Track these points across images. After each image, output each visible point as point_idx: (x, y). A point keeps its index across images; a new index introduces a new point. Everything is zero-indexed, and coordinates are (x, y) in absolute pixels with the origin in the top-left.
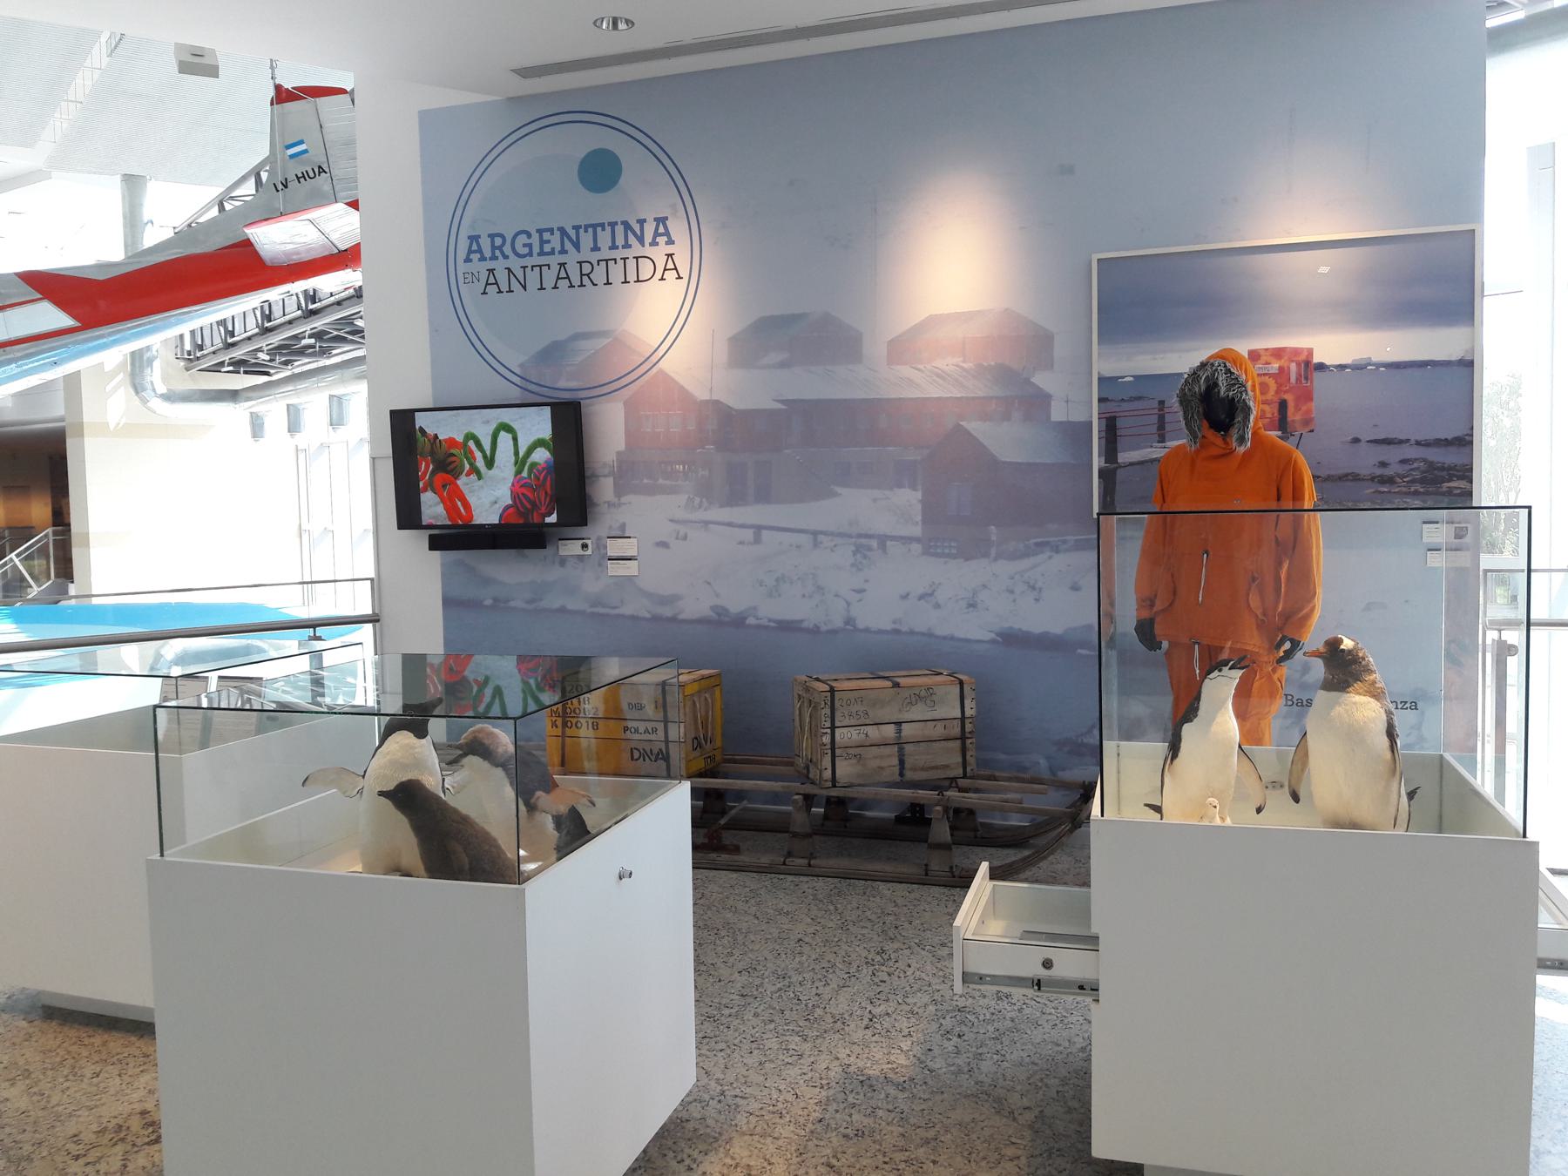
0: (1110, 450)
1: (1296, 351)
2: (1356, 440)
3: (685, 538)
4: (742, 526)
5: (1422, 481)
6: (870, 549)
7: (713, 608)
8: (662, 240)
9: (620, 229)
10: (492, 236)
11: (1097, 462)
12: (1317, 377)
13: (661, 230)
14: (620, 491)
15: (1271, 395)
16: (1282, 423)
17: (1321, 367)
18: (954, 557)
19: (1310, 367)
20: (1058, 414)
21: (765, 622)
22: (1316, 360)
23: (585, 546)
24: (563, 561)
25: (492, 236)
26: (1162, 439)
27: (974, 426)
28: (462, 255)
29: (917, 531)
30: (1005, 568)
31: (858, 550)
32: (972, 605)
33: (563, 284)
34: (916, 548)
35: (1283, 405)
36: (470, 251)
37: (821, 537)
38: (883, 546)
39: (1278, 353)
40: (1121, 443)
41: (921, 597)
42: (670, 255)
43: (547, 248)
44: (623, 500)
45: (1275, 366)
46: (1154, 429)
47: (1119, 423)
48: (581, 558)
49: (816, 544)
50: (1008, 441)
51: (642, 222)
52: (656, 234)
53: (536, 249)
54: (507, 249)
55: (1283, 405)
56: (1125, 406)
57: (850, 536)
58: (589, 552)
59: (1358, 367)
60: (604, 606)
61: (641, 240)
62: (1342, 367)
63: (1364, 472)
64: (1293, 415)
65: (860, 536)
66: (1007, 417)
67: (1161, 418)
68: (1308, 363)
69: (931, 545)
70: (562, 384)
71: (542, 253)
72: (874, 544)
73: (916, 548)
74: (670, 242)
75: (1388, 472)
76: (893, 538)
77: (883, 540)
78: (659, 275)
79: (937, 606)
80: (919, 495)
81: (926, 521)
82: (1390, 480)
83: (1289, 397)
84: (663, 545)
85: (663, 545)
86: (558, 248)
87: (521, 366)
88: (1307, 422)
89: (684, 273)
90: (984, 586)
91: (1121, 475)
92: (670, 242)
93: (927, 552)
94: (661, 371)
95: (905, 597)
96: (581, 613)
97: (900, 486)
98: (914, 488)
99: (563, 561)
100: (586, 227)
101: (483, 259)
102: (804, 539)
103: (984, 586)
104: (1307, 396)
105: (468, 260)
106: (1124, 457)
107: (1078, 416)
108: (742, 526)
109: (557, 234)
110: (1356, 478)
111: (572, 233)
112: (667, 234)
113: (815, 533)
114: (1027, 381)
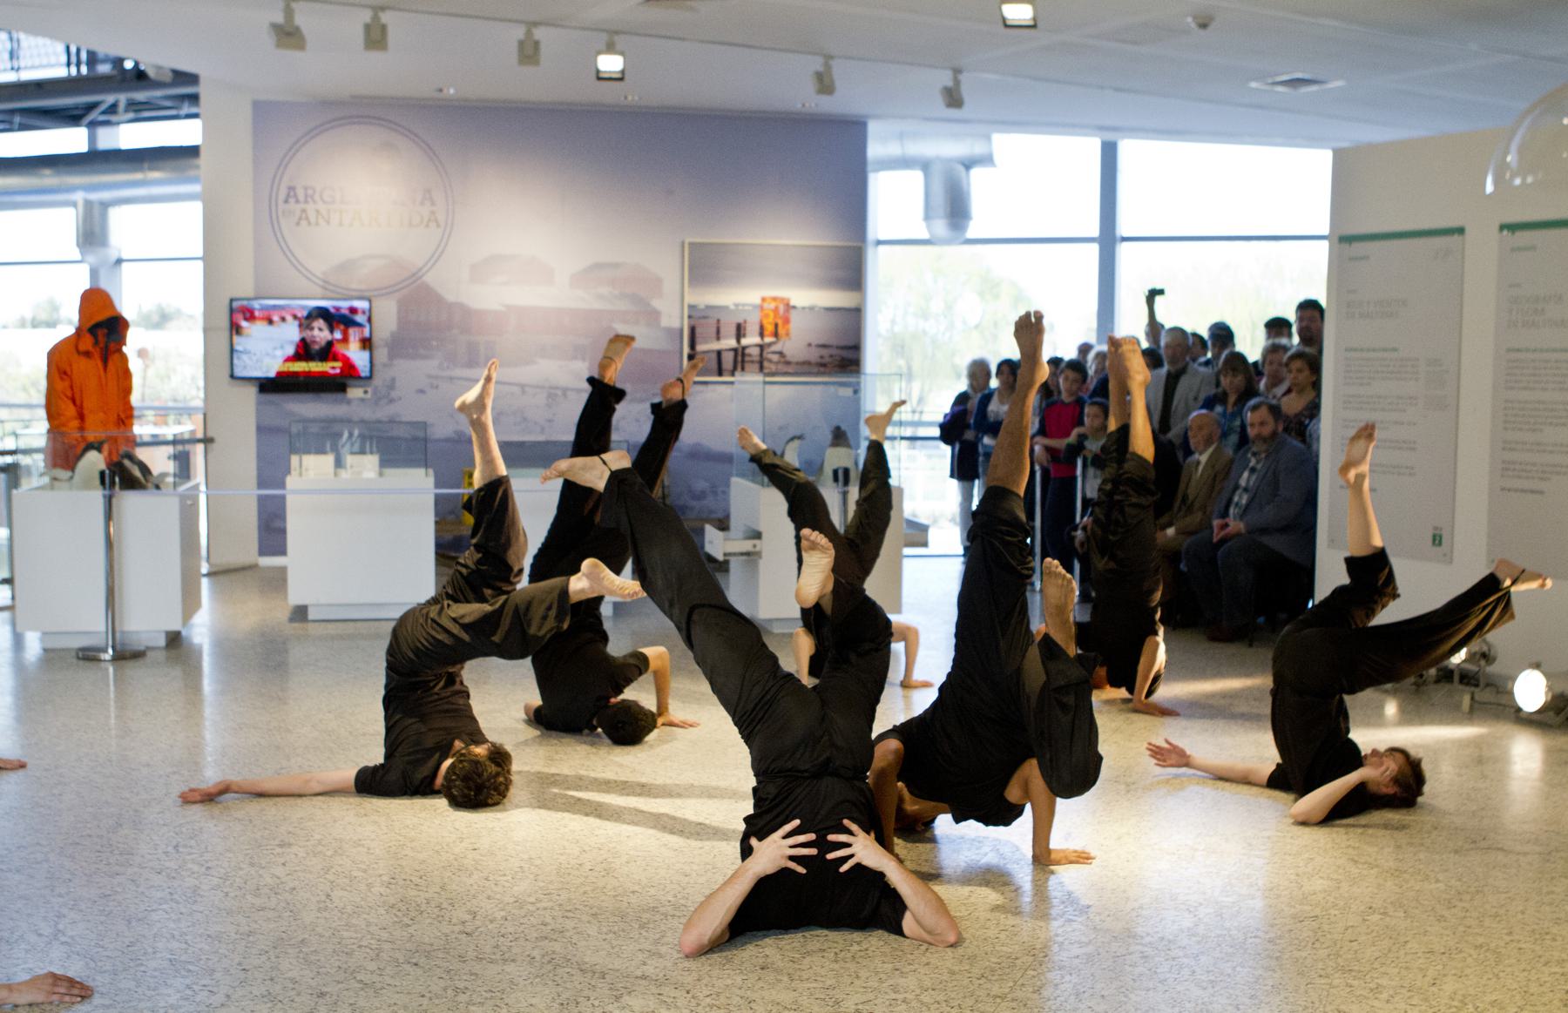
0: (692, 345)
1: (782, 300)
7: (456, 432)
10: (306, 189)
11: (686, 350)
14: (392, 356)
15: (771, 319)
16: (776, 334)
19: (789, 307)
24: (349, 402)
25: (306, 189)
26: (718, 338)
28: (282, 197)
35: (776, 326)
36: (288, 196)
38: (565, 395)
39: (775, 299)
40: (698, 340)
45: (773, 305)
47: (698, 331)
48: (362, 400)
49: (524, 392)
54: (317, 197)
55: (776, 326)
58: (369, 396)
59: (812, 308)
64: (781, 331)
70: (354, 286)
77: (565, 391)
82: (824, 365)
83: (780, 322)
84: (422, 391)
85: (422, 391)
88: (787, 334)
97: (575, 358)
98: (584, 359)
99: (349, 402)
101: (297, 201)
104: (787, 321)
105: (286, 201)
106: (700, 348)
107: (676, 324)
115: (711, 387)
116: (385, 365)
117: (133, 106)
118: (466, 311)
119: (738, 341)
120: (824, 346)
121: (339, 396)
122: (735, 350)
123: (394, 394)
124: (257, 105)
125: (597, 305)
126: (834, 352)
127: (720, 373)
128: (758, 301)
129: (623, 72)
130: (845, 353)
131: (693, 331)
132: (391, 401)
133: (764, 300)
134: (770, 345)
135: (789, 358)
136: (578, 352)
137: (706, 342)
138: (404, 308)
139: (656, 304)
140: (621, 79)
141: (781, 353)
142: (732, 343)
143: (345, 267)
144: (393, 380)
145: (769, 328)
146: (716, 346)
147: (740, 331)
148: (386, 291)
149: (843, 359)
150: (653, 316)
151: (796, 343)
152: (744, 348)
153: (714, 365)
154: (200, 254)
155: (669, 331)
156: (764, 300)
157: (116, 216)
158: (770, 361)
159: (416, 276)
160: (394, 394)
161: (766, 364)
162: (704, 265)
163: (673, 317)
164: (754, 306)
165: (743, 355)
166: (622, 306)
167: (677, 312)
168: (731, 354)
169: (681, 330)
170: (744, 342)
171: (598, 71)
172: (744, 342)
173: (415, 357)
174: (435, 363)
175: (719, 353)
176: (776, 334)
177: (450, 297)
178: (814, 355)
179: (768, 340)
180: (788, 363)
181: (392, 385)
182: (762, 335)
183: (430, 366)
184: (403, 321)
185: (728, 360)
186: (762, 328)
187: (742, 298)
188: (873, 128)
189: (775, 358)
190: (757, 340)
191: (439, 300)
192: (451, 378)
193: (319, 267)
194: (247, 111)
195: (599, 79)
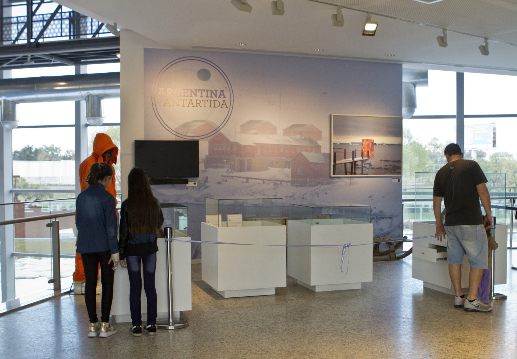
0: (335, 161)
1: (371, 140)
2: (381, 160)
3: (226, 181)
4: (243, 178)
5: (393, 169)
6: (278, 184)
8: (222, 96)
9: (209, 92)
12: (375, 146)
13: (222, 94)
14: (206, 167)
15: (366, 149)
16: (368, 156)
17: (375, 144)
18: (299, 186)
19: (374, 144)
20: (323, 151)
21: (249, 205)
22: (374, 142)
23: (195, 184)
24: (187, 188)
26: (345, 158)
27: (304, 153)
29: (290, 179)
30: (311, 189)
31: (275, 184)
32: (303, 199)
33: (191, 106)
34: (290, 184)
35: (368, 152)
37: (265, 181)
38: (281, 184)
39: (367, 140)
40: (337, 159)
41: (291, 197)
42: (224, 101)
43: (186, 95)
44: (208, 170)
45: (367, 143)
46: (343, 156)
47: (337, 154)
48: (193, 187)
49: (264, 183)
50: (311, 157)
51: (216, 91)
52: (220, 95)
53: (183, 95)
55: (368, 152)
56: (338, 150)
57: (272, 180)
58: (196, 185)
59: (382, 144)
60: (200, 202)
61: (216, 96)
62: (379, 144)
63: (383, 167)
64: (370, 154)
65: (275, 181)
66: (311, 151)
67: (345, 153)
68: (373, 143)
69: (293, 183)
70: (189, 135)
71: (184, 96)
72: (279, 183)
73: (290, 184)
74: (224, 97)
75: (387, 167)
76: (284, 181)
77: (281, 181)
78: (221, 106)
79: (295, 199)
80: (290, 170)
81: (292, 177)
83: (369, 150)
84: (220, 183)
85: (220, 183)
86: (190, 95)
87: (176, 129)
88: (373, 156)
89: (228, 106)
90: (306, 194)
91: (337, 166)
92: (224, 97)
93: (292, 185)
94: (221, 134)
95: (287, 197)
96: (193, 204)
97: (286, 167)
98: (289, 168)
100: (199, 90)
102: (261, 181)
103: (306, 194)
104: (372, 150)
106: (337, 162)
107: (327, 152)
108: (243, 178)
109: (190, 91)
110: (381, 168)
111: (194, 91)
112: (223, 95)
113: (263, 180)
114: (316, 143)
115: (342, 179)
116: (203, 171)
117: (33, 58)
118: (239, 146)
119: (353, 159)
120: (387, 161)
121: (183, 185)
122: (352, 163)
123: (207, 184)
124: (146, 51)
125: (295, 144)
126: (391, 163)
127: (346, 174)
128: (361, 141)
129: (375, 32)
130: (396, 164)
131: (335, 154)
132: (206, 187)
133: (363, 140)
134: (366, 160)
135: (373, 167)
136: (287, 164)
137: (340, 160)
138: (211, 143)
139: (319, 143)
140: (373, 35)
141: (370, 164)
142: (351, 160)
143: (186, 125)
144: (207, 178)
145: (365, 153)
146: (344, 161)
147: (354, 155)
148: (205, 137)
149: (394, 166)
150: (319, 147)
151: (375, 161)
152: (356, 162)
153: (344, 170)
154: (119, 121)
155: (324, 154)
156: (363, 140)
157: (19, 107)
158: (366, 168)
159: (217, 130)
160: (207, 184)
161: (364, 169)
162: (339, 125)
163: (325, 149)
164: (359, 143)
165: (355, 165)
166: (305, 144)
167: (328, 147)
168: (351, 164)
169: (330, 154)
170: (356, 159)
171: (364, 31)
172: (356, 159)
173: (217, 167)
174: (226, 170)
175: (345, 164)
176: (368, 156)
177: (232, 140)
178: (383, 165)
179: (365, 158)
180: (374, 168)
181: (206, 180)
182: (362, 156)
183: (223, 171)
184: (211, 151)
185: (349, 166)
186: (362, 153)
187: (354, 140)
188: (405, 66)
189: (368, 166)
190: (360, 158)
191: (227, 140)
192: (232, 177)
193: (174, 126)
194: (142, 52)
195: (363, 34)
